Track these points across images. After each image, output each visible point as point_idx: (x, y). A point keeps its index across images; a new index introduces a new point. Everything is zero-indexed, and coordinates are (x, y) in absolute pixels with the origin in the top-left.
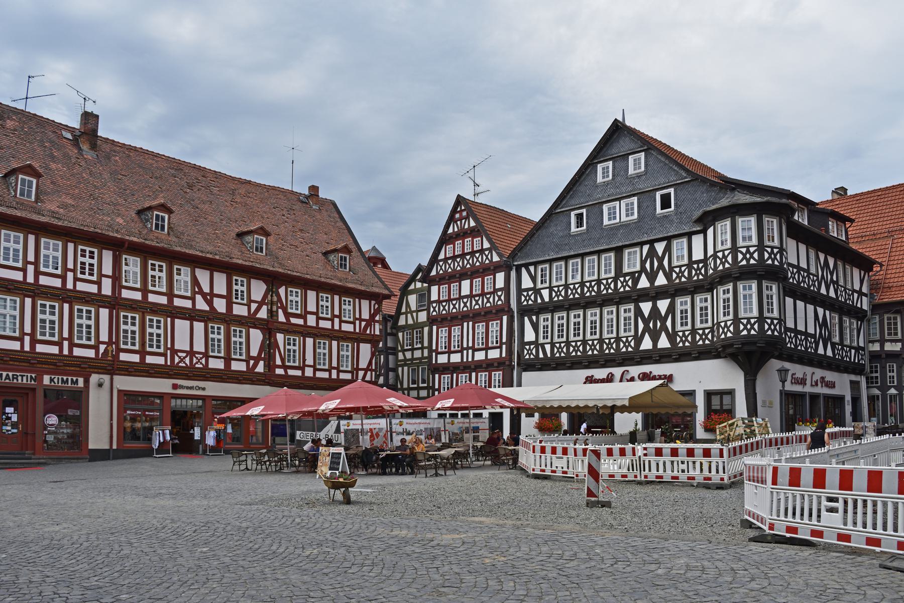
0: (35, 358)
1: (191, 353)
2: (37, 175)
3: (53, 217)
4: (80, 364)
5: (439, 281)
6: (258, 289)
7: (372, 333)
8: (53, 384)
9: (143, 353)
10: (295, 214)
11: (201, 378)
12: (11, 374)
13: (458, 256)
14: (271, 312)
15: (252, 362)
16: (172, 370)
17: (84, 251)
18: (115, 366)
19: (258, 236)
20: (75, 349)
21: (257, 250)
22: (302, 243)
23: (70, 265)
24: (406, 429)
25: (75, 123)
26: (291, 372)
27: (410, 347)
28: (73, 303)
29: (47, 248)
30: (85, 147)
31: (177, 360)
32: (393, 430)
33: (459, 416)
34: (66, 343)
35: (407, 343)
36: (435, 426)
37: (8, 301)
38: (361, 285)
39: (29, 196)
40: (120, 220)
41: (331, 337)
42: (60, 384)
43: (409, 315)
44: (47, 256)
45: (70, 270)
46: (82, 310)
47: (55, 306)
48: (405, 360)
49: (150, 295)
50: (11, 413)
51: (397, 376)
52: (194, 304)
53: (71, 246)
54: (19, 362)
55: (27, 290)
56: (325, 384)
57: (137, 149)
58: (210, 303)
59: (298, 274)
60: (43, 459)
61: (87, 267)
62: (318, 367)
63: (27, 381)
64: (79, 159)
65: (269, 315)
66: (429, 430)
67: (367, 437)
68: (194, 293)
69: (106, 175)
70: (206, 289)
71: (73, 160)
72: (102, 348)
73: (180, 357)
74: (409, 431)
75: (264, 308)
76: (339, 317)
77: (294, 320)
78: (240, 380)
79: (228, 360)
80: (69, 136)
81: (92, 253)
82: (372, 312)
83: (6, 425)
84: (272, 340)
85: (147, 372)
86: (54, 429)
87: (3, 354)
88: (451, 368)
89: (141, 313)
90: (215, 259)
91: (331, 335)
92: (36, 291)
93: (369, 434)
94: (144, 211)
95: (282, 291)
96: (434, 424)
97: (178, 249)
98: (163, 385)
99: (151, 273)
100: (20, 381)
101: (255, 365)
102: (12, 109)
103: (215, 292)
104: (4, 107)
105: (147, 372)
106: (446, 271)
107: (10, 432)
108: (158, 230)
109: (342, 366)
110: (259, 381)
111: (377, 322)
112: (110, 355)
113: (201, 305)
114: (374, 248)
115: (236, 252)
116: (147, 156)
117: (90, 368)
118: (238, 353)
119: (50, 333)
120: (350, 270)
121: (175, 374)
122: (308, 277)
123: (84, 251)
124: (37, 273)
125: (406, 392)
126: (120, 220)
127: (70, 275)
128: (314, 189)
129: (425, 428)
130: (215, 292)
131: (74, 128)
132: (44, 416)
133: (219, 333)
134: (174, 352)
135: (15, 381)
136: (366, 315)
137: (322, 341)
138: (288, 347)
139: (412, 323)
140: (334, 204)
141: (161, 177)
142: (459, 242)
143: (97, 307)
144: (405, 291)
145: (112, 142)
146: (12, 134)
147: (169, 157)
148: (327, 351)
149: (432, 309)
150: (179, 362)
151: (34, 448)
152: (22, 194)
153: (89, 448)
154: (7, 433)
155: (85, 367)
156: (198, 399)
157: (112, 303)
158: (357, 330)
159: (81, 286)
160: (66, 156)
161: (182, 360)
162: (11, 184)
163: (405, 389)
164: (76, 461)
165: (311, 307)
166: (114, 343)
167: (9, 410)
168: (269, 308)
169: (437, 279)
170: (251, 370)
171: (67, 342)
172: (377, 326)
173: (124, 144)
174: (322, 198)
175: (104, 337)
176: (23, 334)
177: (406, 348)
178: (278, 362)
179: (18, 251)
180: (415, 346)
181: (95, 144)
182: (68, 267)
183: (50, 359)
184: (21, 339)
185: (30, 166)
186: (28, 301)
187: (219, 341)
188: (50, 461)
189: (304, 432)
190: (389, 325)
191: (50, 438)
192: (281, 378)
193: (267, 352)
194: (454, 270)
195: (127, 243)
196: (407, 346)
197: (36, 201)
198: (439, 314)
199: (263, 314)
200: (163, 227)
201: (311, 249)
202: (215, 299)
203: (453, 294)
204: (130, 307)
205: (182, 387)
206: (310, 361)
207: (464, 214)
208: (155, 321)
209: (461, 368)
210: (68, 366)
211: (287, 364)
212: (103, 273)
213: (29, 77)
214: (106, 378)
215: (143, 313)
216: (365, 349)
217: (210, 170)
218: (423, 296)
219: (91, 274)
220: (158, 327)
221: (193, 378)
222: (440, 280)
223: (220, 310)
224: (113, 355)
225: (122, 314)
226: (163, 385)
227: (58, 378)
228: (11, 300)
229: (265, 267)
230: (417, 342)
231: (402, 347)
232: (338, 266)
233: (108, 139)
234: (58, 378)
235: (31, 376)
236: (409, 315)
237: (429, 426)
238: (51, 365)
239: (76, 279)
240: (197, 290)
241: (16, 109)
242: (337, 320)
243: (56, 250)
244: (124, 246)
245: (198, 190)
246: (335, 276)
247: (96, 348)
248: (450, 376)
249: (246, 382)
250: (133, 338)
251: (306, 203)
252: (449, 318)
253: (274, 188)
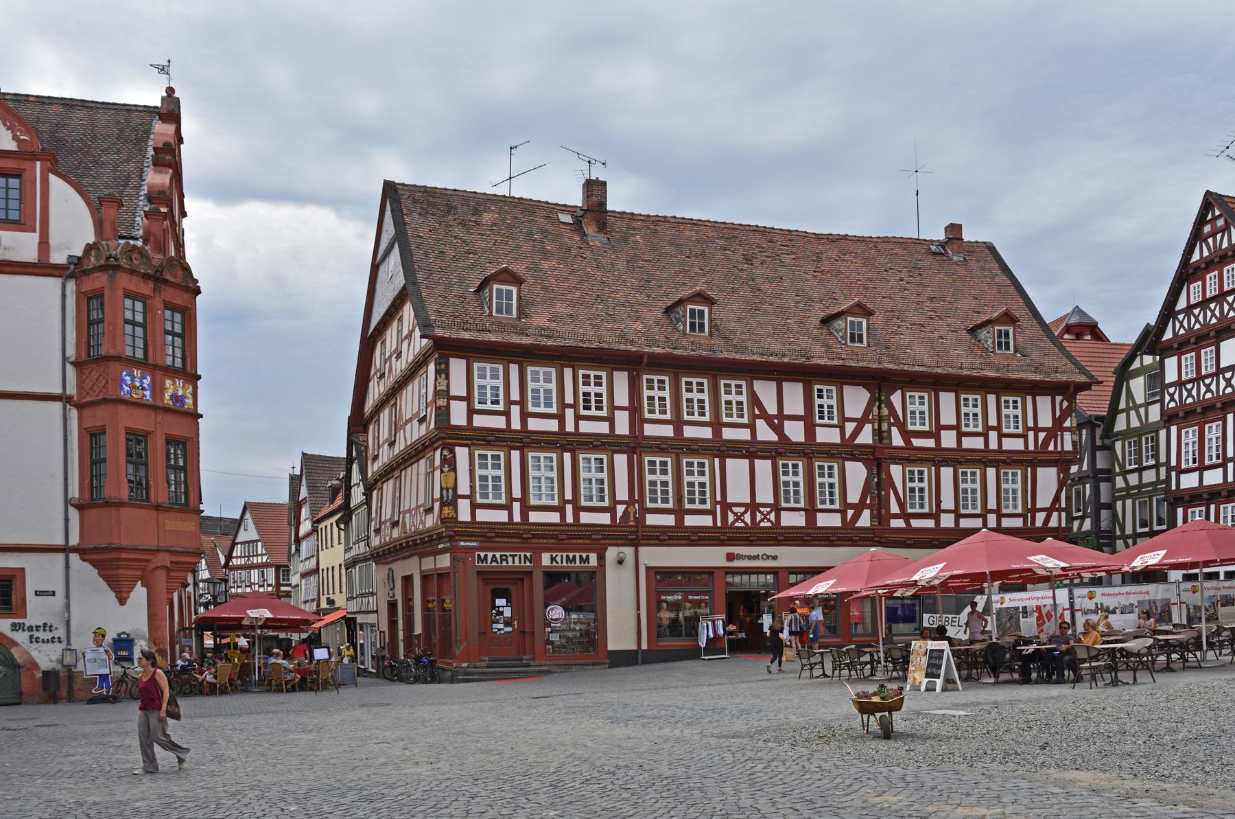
1: (753, 506)
2: (518, 281)
3: (541, 335)
5: (1178, 349)
6: (856, 400)
7: (1059, 449)
8: (554, 564)
9: (679, 512)
10: (920, 275)
11: (771, 542)
12: (498, 555)
13: (1212, 299)
14: (879, 434)
15: (850, 513)
16: (723, 534)
17: (588, 377)
18: (640, 534)
19: (853, 319)
20: (582, 514)
21: (853, 340)
22: (931, 318)
23: (569, 399)
24: (1102, 604)
25: (576, 198)
26: (916, 523)
27: (1136, 466)
28: (577, 451)
29: (536, 380)
30: (590, 230)
31: (731, 518)
32: (1077, 607)
33: (1222, 577)
34: (569, 508)
35: (1130, 460)
36: (1159, 597)
37: (542, 459)
38: (1035, 372)
39: (509, 311)
40: (639, 326)
41: (984, 463)
42: (565, 564)
43: (1133, 413)
44: (536, 391)
45: (570, 406)
46: (486, 455)
47: (499, 456)
48: (1128, 487)
49: (685, 428)
50: (503, 607)
51: (1115, 515)
52: (753, 434)
53: (568, 373)
54: (508, 537)
55: (512, 440)
56: (924, 538)
57: (667, 219)
58: (779, 430)
59: (921, 369)
60: (546, 665)
61: (593, 398)
62: (963, 511)
63: (520, 563)
64: (581, 248)
65: (877, 438)
66: (1147, 603)
67: (1032, 620)
68: (754, 417)
69: (621, 265)
70: (772, 409)
71: (574, 252)
72: (620, 509)
73: (735, 514)
74: (1108, 608)
75: (868, 428)
76: (998, 428)
77: (917, 442)
78: (833, 541)
79: (811, 512)
80: (566, 218)
81: (598, 377)
82: (1058, 414)
83: (497, 622)
84: (883, 476)
85: (687, 538)
86: (559, 625)
87: (487, 528)
88: (1206, 496)
89: (674, 456)
90: (783, 363)
91: (983, 459)
92: (525, 440)
93: (1036, 615)
94: (676, 307)
95: (896, 398)
96: (1156, 593)
97: (725, 355)
98: (711, 557)
99: (685, 395)
100: (510, 563)
101: (856, 517)
102: (490, 197)
103: (786, 412)
104: (480, 196)
105: (687, 538)
106: (1190, 329)
107: (502, 632)
108: (695, 332)
109: (1007, 507)
110: (863, 540)
111: (1068, 429)
112: (632, 519)
113: (765, 433)
114: (1077, 310)
115: (818, 348)
116: (682, 227)
117: (604, 539)
118: (828, 501)
120: (1016, 351)
121: (730, 539)
122: (940, 371)
123: (588, 377)
124: (525, 416)
125: (1130, 541)
126: (639, 326)
127: (569, 413)
128: (954, 230)
129: (1139, 602)
130: (786, 412)
131: (576, 207)
132: (546, 607)
133: (795, 474)
134: (727, 506)
135: (504, 563)
136: (1046, 421)
137: (969, 471)
138: (909, 485)
139: (1139, 425)
140: (991, 249)
141: (703, 254)
142: (1212, 275)
143: (609, 453)
144: (1124, 373)
145: (630, 216)
146: (490, 230)
147: (716, 222)
148: (978, 486)
149: (1167, 398)
150: (736, 521)
151: (533, 652)
152: (499, 311)
153: (609, 649)
154: (498, 633)
155: (598, 539)
156: (766, 573)
157: (631, 445)
158: (1031, 447)
159: (586, 427)
160: (565, 248)
161: (739, 517)
162: (485, 298)
163: (1129, 536)
164: (591, 667)
165: (948, 417)
166: (637, 501)
167: (500, 602)
168: (876, 427)
169: (1176, 346)
170: (848, 525)
171: (519, 503)
172: (1068, 437)
173: (649, 216)
174: (970, 242)
175: (622, 493)
176: (511, 500)
177: (1128, 468)
178: (894, 508)
179: (497, 388)
180: (1145, 464)
181: (605, 224)
183: (549, 531)
184: (508, 507)
185: (506, 270)
186: (516, 455)
187: (796, 484)
188: (555, 668)
189: (935, 615)
190: (1098, 432)
191: (555, 637)
192: (902, 534)
193: (875, 495)
194: (1206, 325)
195: (646, 357)
196: (1130, 465)
197: (519, 318)
198: (1182, 405)
199: (866, 437)
200: (702, 326)
201: (949, 325)
202: (786, 423)
203: (1206, 367)
204: (659, 448)
205: (740, 557)
206: (948, 502)
207: (1220, 223)
208: (790, 466)
209: (1224, 493)
210: (574, 539)
211: (909, 511)
212: (615, 404)
213: (511, 148)
214: (628, 551)
215: (678, 455)
216: (1048, 478)
217: (781, 230)
218: (1156, 378)
219: (599, 408)
220: (702, 473)
221: (699, 542)
222: (1180, 346)
223: (794, 440)
224: (636, 519)
225: (647, 459)
226: (711, 557)
227: (562, 556)
228: (545, 457)
229: (865, 365)
230: (1147, 457)
231: (1122, 466)
232: (994, 347)
233: (624, 213)
234: (562, 556)
235: (525, 555)
236: (1133, 413)
237: (1147, 598)
238: (550, 538)
239: (578, 418)
240: (757, 412)
241: (495, 195)
242: (993, 435)
243: (547, 380)
244: (642, 362)
245: (762, 263)
246: (989, 364)
247: (611, 510)
248: (1203, 508)
249: (843, 543)
250: (665, 492)
251: (942, 254)
252: (1199, 410)
253: (886, 240)
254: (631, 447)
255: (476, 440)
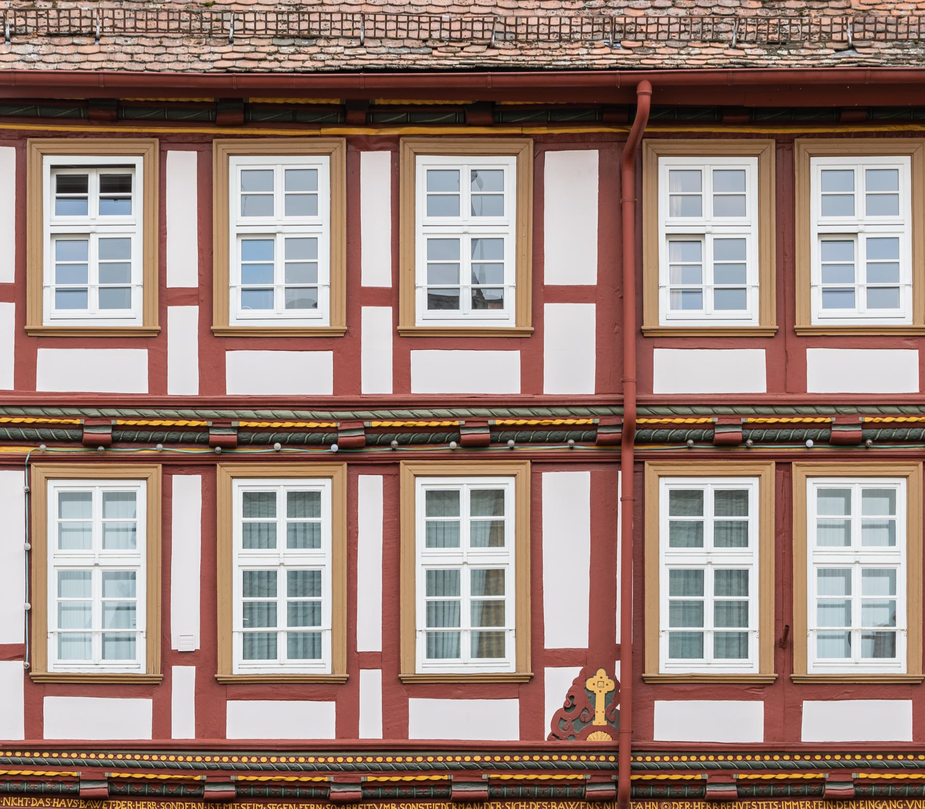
0: (220, 774)
4: (448, 784)
28: (406, 470)
89: (769, 470)
112: (600, 719)
119: (293, 638)
143: (525, 469)
157: (604, 434)
182: (367, 281)
215: (784, 464)
254: (602, 443)
255: (49, 441)
